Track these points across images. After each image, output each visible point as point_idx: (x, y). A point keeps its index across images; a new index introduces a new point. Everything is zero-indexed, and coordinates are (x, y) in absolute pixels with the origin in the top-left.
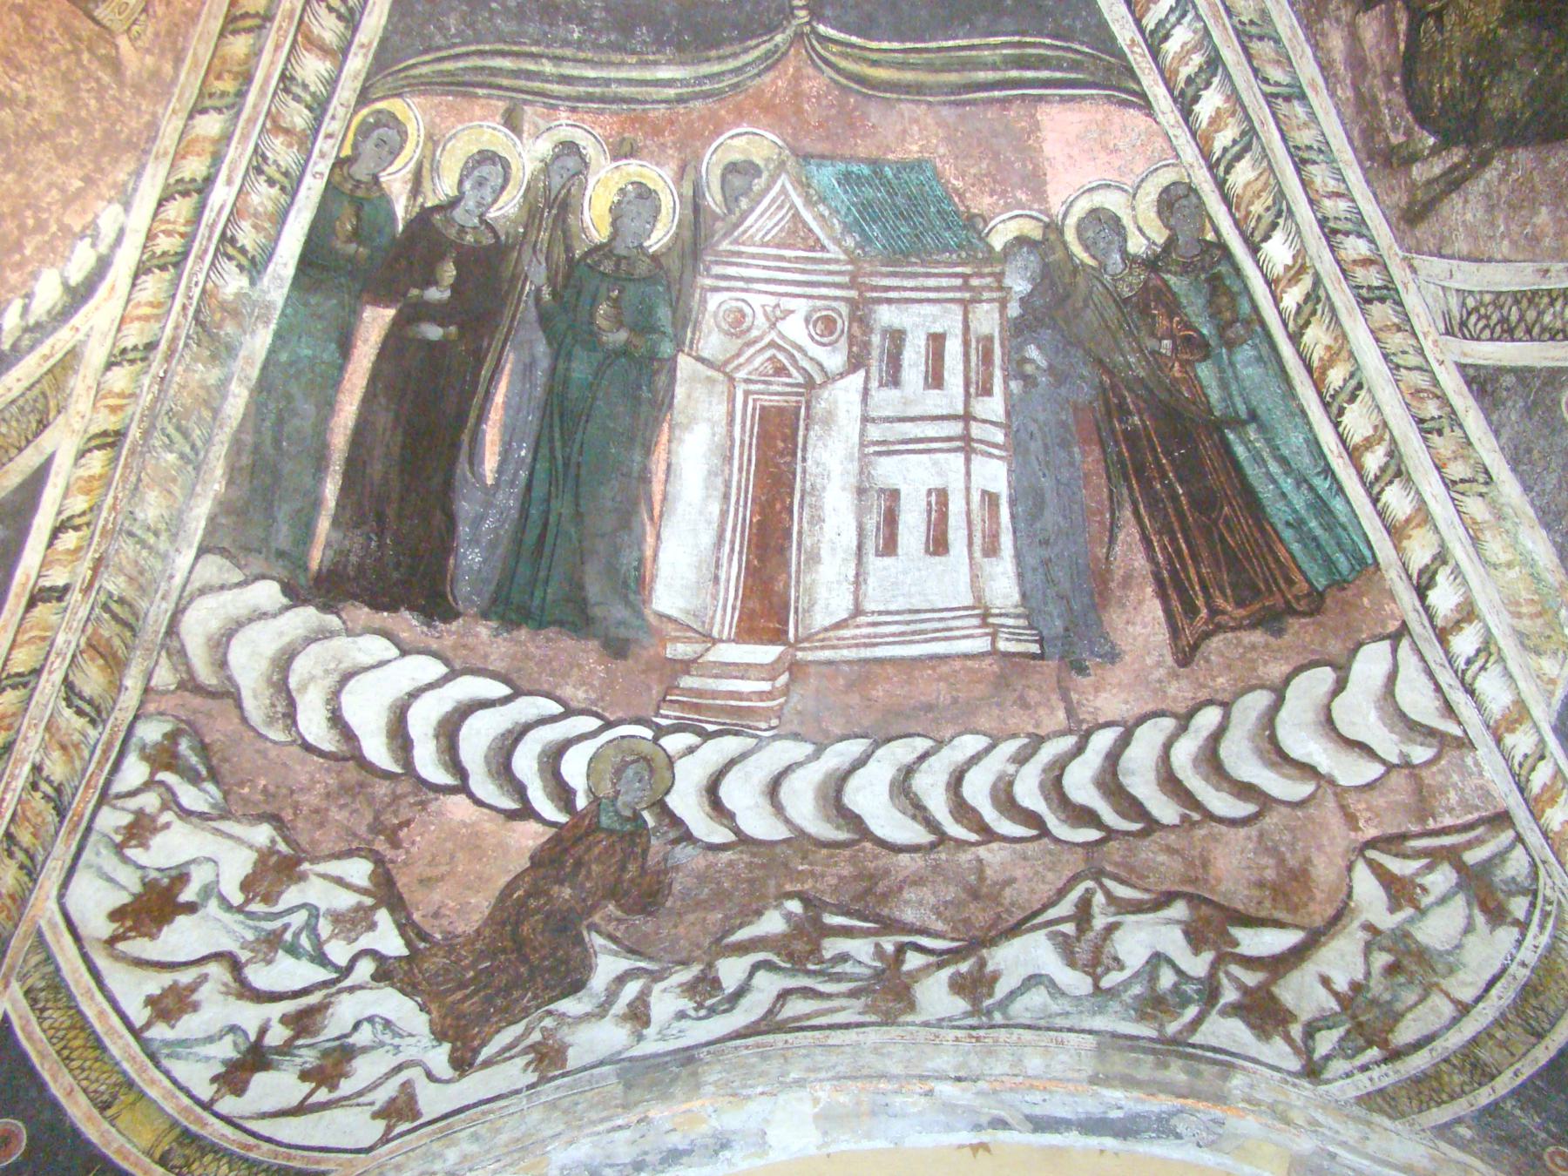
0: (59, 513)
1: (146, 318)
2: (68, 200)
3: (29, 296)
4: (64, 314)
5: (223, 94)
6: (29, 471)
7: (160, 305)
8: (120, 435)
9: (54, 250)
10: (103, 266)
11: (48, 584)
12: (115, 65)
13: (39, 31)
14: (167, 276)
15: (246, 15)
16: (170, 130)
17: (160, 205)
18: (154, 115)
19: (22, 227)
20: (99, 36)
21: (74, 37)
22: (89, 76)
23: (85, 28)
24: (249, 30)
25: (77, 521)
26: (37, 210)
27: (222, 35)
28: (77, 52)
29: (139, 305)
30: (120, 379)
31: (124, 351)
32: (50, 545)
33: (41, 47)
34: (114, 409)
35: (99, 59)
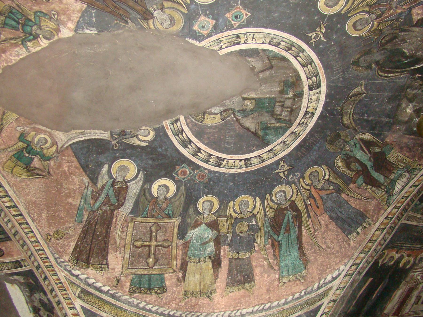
1: (344, 283)
2: (336, 264)
3: (326, 278)
4: (331, 282)
8: (336, 300)
10: (339, 274)
12: (349, 244)
15: (372, 240)
17: (351, 266)
19: (327, 268)
21: (344, 239)
22: (344, 245)
23: (346, 238)
26: (330, 265)
27: (368, 242)
28: (343, 242)
30: (338, 292)
34: (336, 296)
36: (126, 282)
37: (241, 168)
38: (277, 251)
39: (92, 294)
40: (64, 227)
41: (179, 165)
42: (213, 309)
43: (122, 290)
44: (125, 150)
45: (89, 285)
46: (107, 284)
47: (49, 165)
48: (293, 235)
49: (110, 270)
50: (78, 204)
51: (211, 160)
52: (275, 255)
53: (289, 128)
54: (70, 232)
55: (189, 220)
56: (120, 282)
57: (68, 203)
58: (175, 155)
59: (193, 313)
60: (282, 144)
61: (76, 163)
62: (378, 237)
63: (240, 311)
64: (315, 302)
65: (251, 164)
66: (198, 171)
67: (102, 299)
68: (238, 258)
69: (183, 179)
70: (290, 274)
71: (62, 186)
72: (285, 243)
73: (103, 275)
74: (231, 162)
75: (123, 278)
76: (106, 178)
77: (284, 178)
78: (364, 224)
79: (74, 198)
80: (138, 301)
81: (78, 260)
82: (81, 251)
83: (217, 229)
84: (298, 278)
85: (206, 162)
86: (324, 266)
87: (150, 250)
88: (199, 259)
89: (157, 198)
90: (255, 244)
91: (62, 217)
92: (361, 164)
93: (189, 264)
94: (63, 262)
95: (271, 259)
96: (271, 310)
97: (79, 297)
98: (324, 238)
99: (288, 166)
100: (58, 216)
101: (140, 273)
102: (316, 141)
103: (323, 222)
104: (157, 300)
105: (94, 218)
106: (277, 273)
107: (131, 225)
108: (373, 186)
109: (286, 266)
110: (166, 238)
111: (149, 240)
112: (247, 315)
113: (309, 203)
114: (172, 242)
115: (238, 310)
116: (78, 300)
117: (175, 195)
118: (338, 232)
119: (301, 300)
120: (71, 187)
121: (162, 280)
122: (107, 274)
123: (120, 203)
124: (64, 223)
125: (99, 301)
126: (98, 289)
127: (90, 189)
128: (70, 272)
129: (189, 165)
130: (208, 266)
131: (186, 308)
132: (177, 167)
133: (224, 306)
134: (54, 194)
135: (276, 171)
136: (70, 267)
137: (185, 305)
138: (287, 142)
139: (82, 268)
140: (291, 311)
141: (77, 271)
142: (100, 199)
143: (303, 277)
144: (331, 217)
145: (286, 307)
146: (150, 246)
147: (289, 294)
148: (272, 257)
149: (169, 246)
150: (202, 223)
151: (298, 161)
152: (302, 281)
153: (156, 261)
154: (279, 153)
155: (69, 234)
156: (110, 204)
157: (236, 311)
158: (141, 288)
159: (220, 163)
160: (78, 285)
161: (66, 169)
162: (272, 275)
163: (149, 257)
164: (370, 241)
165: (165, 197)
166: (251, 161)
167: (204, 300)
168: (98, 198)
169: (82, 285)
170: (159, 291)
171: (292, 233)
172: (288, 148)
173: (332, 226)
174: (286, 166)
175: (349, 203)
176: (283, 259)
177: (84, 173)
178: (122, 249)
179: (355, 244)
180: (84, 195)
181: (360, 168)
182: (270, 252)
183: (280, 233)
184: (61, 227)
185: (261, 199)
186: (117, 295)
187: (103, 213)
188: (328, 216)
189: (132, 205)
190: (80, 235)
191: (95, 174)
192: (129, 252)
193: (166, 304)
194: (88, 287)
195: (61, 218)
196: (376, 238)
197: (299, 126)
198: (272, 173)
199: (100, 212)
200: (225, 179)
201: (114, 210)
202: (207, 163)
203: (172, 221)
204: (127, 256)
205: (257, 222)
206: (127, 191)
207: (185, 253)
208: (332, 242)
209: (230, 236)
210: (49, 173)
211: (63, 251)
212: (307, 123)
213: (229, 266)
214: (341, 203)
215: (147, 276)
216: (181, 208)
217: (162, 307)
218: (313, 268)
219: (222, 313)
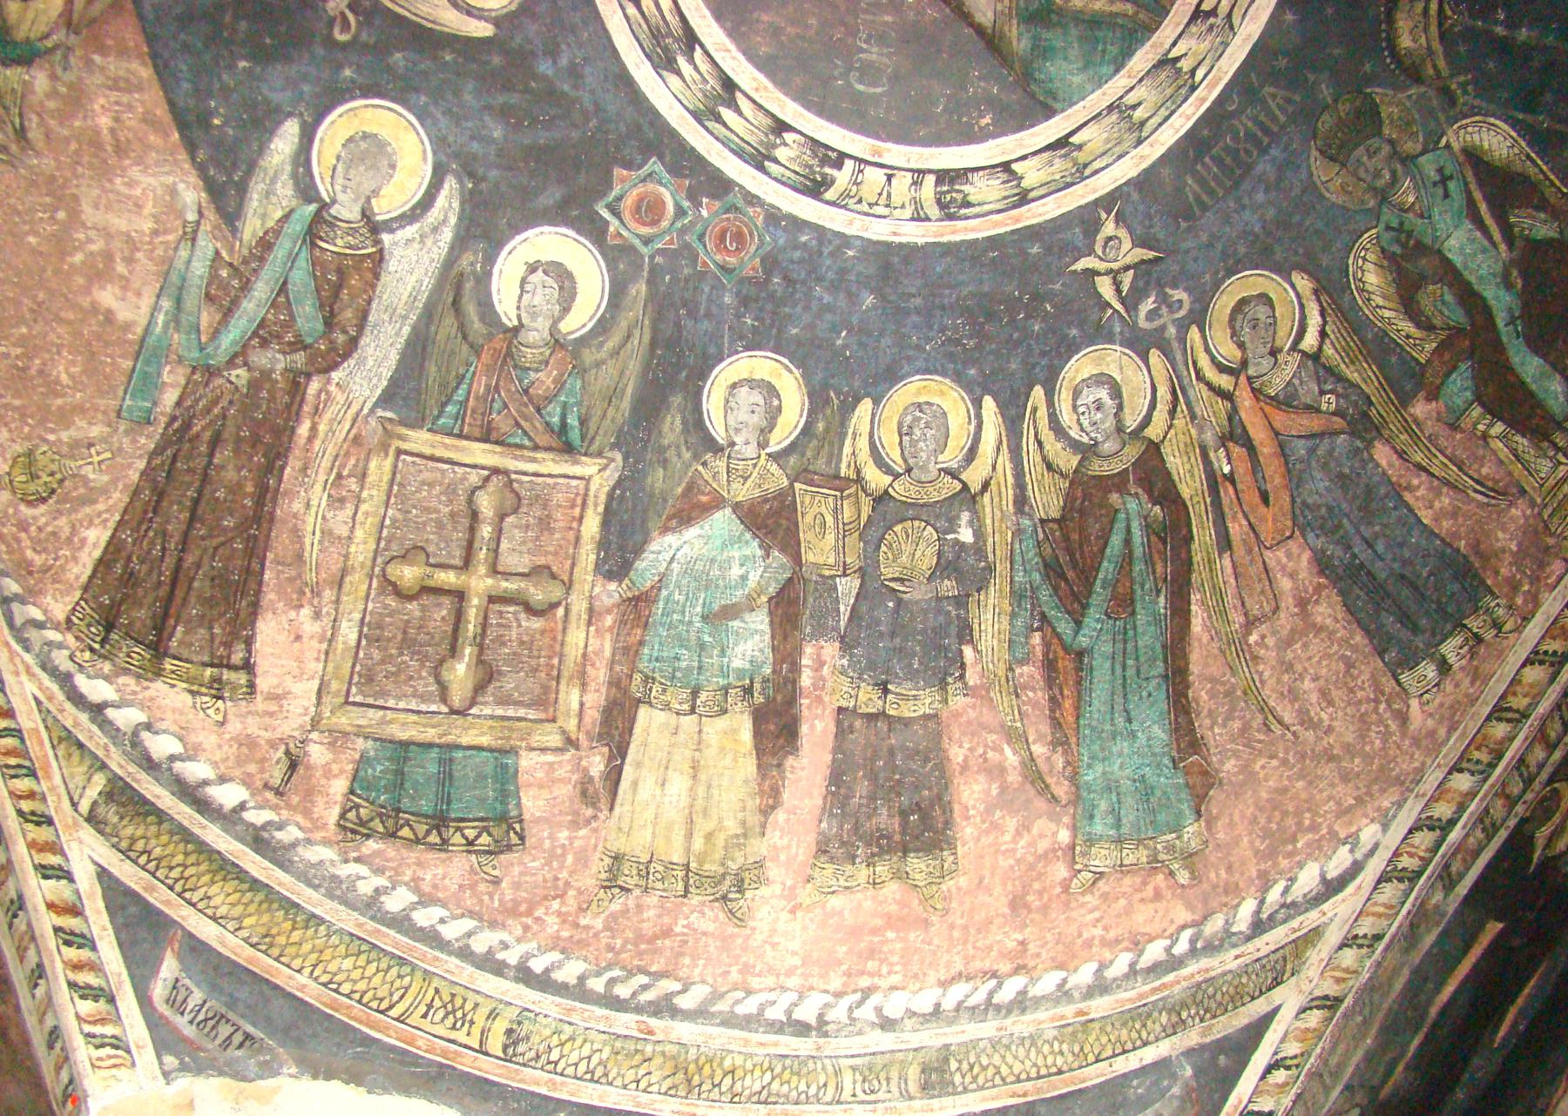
0: (1276, 1053)
1: (1379, 915)
2: (1343, 812)
3: (1292, 880)
4: (1316, 900)
5: (1478, 762)
6: (1256, 1016)
7: (1391, 907)
8: (1338, 1000)
9: (1320, 848)
10: (1356, 869)
11: (1256, 1109)
12: (1403, 718)
13: (1354, 678)
14: (1402, 886)
15: (1510, 709)
16: (1432, 778)
17: (1410, 832)
18: (1423, 764)
19: (1299, 823)
20: (1398, 694)
21: (1379, 690)
22: (1381, 721)
23: (1389, 685)
24: (1509, 721)
25: (1289, 1062)
26: (1315, 814)
27: (1488, 719)
28: (1377, 701)
29: (1375, 904)
30: (1349, 957)
31: (1356, 937)
32: (1263, 1077)
33: (1351, 691)
34: (1338, 981)
35: (1393, 711)
36: (328, 774)
37: (919, 219)
38: (1068, 704)
39: (161, 816)
40: (65, 436)
41: (629, 165)
42: (746, 969)
43: (307, 813)
44: (381, 50)
45: (149, 764)
46: (237, 773)
47: (28, 87)
48: (1148, 637)
49: (260, 704)
50: (144, 322)
51: (782, 153)
52: (1056, 724)
53: (1151, 29)
54: (88, 471)
55: (657, 479)
56: (301, 770)
57: (95, 308)
58: (613, 103)
59: (644, 979)
60: (1114, 117)
61: (152, 99)
62: (1537, 698)
63: (875, 999)
64: (1238, 998)
65: (968, 205)
66: (717, 204)
67: (203, 848)
68: (882, 714)
69: (647, 241)
70: (1125, 830)
71: (75, 214)
72: (1108, 664)
73: (222, 724)
74: (874, 177)
75: (317, 753)
76: (285, 191)
77: (1118, 307)
78: (1474, 623)
79: (125, 288)
80: (381, 881)
81: (109, 627)
82: (130, 578)
83: (791, 546)
84: (1162, 857)
85: (759, 160)
86: (1285, 813)
87: (459, 616)
88: (695, 693)
89: (516, 330)
90: (968, 651)
91: (57, 382)
92: (1469, 296)
93: (643, 712)
94: (40, 626)
95: (1039, 739)
96: (1028, 1017)
97: (92, 819)
98: (1289, 667)
99: (1135, 246)
100: (41, 372)
101: (404, 735)
102: (1266, 131)
103: (1285, 584)
104: (473, 887)
105: (208, 410)
106: (1066, 819)
107: (379, 468)
108: (1518, 424)
109: (1111, 786)
110: (541, 561)
111: (458, 562)
112: (909, 1023)
113: (1227, 469)
114: (569, 586)
115: (867, 993)
116: (87, 833)
117: (603, 326)
118: (1355, 649)
119: (1170, 977)
120: (120, 223)
121: (505, 779)
122: (243, 720)
123: (341, 338)
124: (65, 418)
125: (186, 854)
126: (191, 794)
127: (206, 245)
128: (65, 680)
129: (675, 170)
130: (732, 732)
131: (610, 948)
132: (618, 172)
133: (797, 961)
134: (34, 252)
135: (1081, 265)
136: (71, 658)
137: (607, 928)
138: (1139, 114)
139: (126, 671)
140: (1124, 1032)
141: (101, 683)
142: (248, 305)
143: (1189, 858)
144: (1322, 564)
145: (1100, 1006)
146: (460, 595)
147: (1117, 941)
148: (1045, 728)
149: (554, 606)
150: (717, 503)
151: (1184, 225)
152: (1183, 877)
153: (486, 676)
154: (1097, 165)
155: (85, 481)
156: (289, 337)
157: (858, 996)
158: (399, 810)
159: (824, 176)
160: (96, 757)
161: (104, 122)
162: (1041, 825)
163: (454, 651)
164: (1499, 711)
165: (554, 330)
166: (966, 188)
167: (702, 917)
168: (235, 302)
169: (118, 762)
170: (485, 839)
171: (1141, 618)
172: (1139, 142)
173: (1327, 611)
174: (1127, 245)
175: (1407, 496)
176: (1096, 747)
177: (183, 156)
178: (328, 594)
179: (1430, 722)
180: (174, 278)
181: (1458, 316)
182: (1035, 705)
183: (1085, 607)
184: (52, 437)
185: (1003, 407)
186: (279, 835)
187: (254, 385)
188: (1306, 555)
189: (394, 357)
190: (136, 493)
191: (235, 166)
192: (357, 616)
193: (512, 911)
194: (143, 775)
195: (53, 388)
196: (1526, 701)
197: (1194, 29)
198: (1060, 274)
199: (240, 375)
200: (843, 272)
201: (309, 376)
202: (761, 168)
203: (577, 470)
204: (349, 633)
205: (979, 534)
206: (377, 276)
207: (629, 653)
208: (1324, 694)
209: (848, 587)
210: (21, 133)
211: (46, 569)
212: (1229, 16)
213: (835, 750)
214: (1369, 491)
215: (434, 753)
216: (626, 404)
217: (493, 925)
218: (1236, 817)
219: (789, 998)
